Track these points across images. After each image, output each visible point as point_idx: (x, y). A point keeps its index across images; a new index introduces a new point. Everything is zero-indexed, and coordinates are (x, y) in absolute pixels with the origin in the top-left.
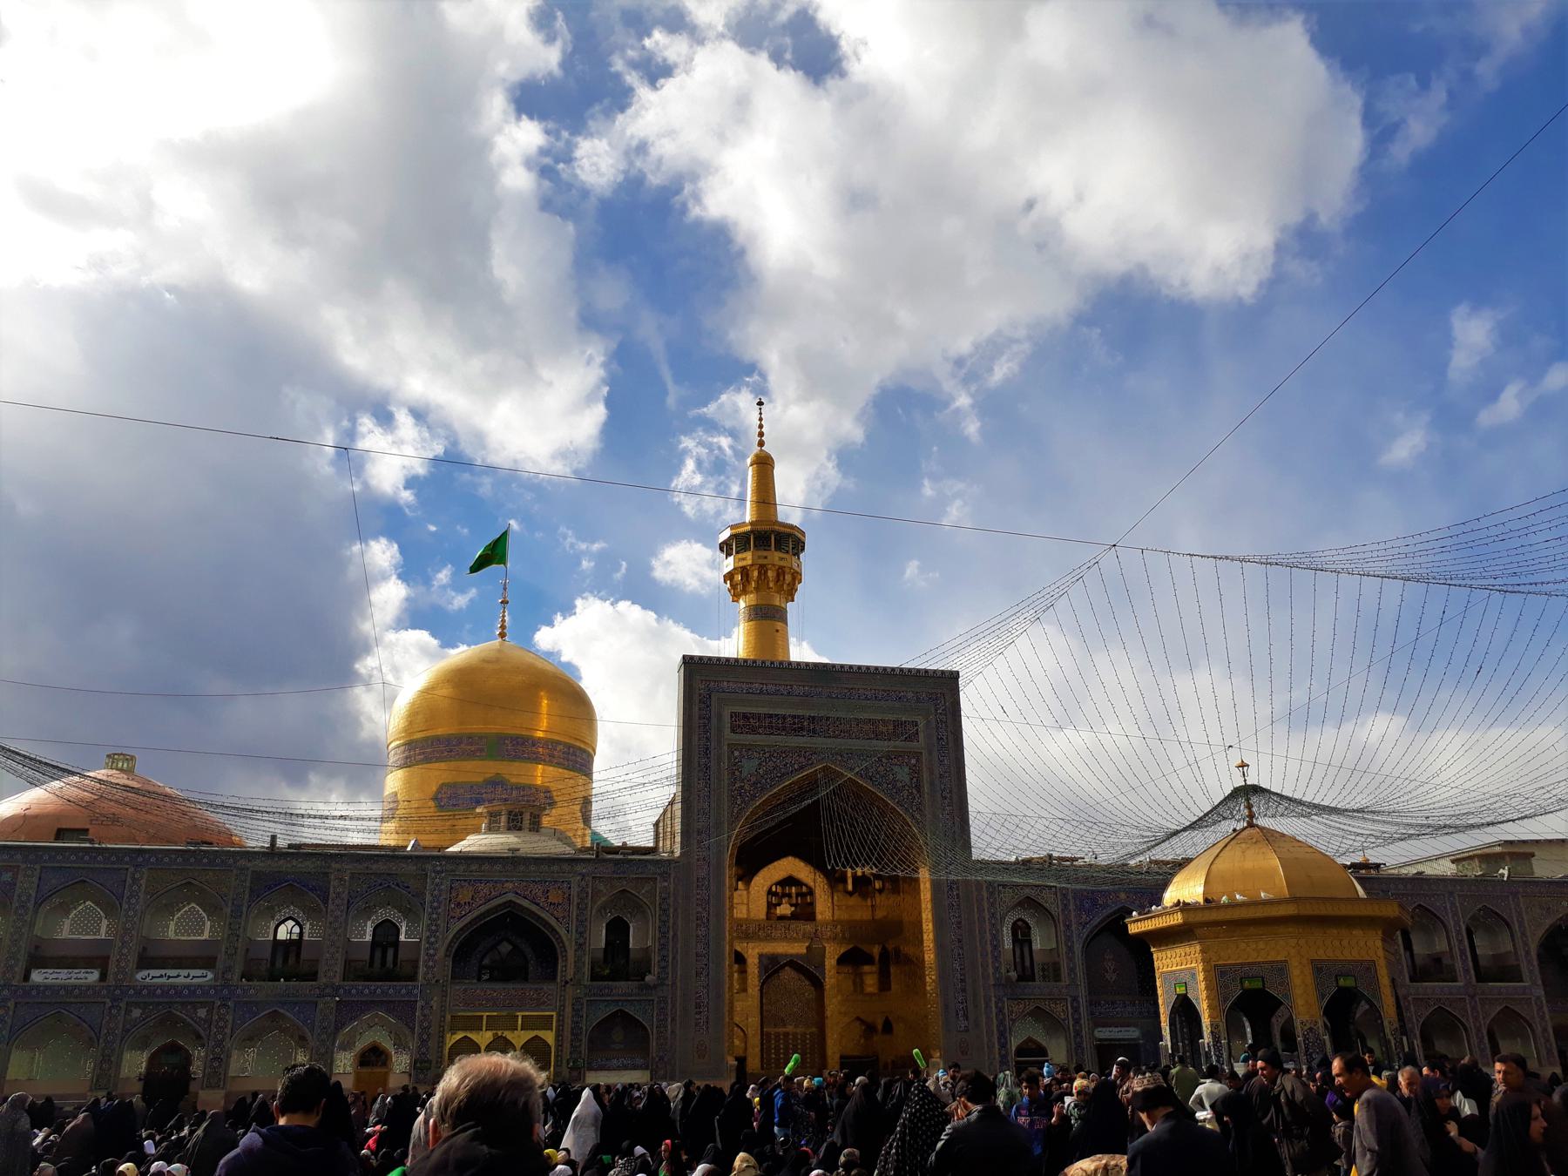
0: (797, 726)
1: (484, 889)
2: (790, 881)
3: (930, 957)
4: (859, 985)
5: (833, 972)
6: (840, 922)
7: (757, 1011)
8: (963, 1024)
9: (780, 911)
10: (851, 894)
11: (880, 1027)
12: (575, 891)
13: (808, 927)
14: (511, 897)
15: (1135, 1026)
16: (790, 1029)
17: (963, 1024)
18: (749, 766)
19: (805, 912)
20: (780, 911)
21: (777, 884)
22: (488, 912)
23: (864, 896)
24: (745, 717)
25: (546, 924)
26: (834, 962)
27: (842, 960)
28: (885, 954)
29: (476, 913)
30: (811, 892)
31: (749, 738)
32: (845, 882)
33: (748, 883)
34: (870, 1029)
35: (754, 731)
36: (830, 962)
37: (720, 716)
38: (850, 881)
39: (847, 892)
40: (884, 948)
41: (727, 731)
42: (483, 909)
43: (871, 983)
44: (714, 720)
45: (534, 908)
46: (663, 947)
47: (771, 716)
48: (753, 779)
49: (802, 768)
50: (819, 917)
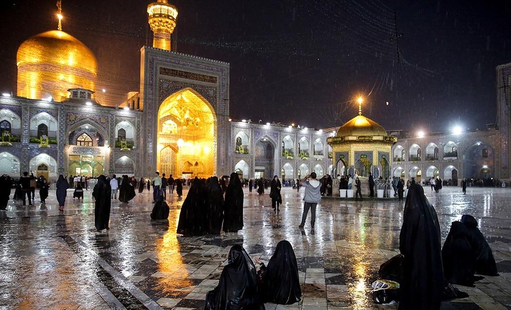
11: (194, 165)
15: (264, 166)
24: (165, 69)
31: (166, 77)
35: (167, 74)
37: (156, 68)
41: (159, 72)
44: (155, 69)
47: (173, 70)
48: (167, 89)
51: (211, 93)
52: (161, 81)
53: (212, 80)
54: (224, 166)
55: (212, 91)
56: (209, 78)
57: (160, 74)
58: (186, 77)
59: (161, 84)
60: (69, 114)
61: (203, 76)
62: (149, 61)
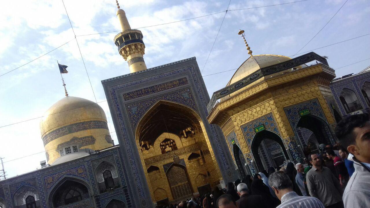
0: (146, 92)
1: (56, 176)
2: (166, 140)
3: (211, 149)
4: (199, 163)
5: (188, 162)
6: (185, 147)
7: (167, 183)
8: (227, 166)
9: (167, 150)
10: (186, 138)
12: (86, 167)
13: (176, 152)
14: (65, 176)
16: (180, 184)
17: (227, 166)
18: (134, 109)
19: (175, 148)
20: (167, 150)
21: (162, 142)
22: (59, 183)
23: (191, 136)
24: (128, 94)
25: (80, 180)
26: (187, 160)
27: (190, 158)
28: (201, 152)
29: (55, 185)
30: (174, 141)
31: (132, 100)
32: (184, 135)
33: (153, 145)
34: (205, 176)
35: (132, 97)
36: (186, 160)
37: (120, 97)
38: (185, 134)
39: (185, 137)
40: (201, 151)
42: (57, 183)
43: (201, 161)
45: (74, 177)
46: (121, 175)
47: (137, 91)
49: (152, 104)
50: (178, 148)
51: (186, 95)
52: (129, 107)
53: (182, 82)
54: (229, 168)
55: (187, 94)
56: (178, 82)
57: (125, 100)
58: (153, 91)
59: (130, 110)
60: (46, 178)
61: (171, 82)
62: (110, 93)
